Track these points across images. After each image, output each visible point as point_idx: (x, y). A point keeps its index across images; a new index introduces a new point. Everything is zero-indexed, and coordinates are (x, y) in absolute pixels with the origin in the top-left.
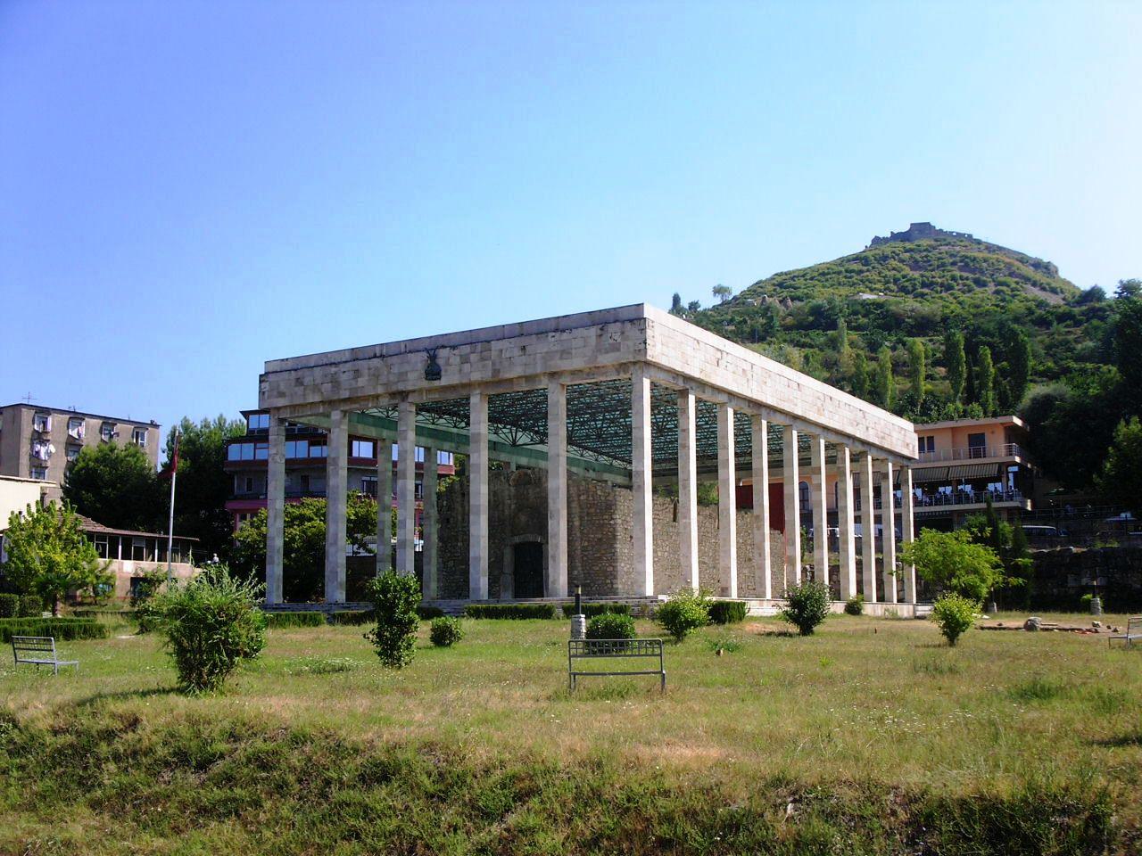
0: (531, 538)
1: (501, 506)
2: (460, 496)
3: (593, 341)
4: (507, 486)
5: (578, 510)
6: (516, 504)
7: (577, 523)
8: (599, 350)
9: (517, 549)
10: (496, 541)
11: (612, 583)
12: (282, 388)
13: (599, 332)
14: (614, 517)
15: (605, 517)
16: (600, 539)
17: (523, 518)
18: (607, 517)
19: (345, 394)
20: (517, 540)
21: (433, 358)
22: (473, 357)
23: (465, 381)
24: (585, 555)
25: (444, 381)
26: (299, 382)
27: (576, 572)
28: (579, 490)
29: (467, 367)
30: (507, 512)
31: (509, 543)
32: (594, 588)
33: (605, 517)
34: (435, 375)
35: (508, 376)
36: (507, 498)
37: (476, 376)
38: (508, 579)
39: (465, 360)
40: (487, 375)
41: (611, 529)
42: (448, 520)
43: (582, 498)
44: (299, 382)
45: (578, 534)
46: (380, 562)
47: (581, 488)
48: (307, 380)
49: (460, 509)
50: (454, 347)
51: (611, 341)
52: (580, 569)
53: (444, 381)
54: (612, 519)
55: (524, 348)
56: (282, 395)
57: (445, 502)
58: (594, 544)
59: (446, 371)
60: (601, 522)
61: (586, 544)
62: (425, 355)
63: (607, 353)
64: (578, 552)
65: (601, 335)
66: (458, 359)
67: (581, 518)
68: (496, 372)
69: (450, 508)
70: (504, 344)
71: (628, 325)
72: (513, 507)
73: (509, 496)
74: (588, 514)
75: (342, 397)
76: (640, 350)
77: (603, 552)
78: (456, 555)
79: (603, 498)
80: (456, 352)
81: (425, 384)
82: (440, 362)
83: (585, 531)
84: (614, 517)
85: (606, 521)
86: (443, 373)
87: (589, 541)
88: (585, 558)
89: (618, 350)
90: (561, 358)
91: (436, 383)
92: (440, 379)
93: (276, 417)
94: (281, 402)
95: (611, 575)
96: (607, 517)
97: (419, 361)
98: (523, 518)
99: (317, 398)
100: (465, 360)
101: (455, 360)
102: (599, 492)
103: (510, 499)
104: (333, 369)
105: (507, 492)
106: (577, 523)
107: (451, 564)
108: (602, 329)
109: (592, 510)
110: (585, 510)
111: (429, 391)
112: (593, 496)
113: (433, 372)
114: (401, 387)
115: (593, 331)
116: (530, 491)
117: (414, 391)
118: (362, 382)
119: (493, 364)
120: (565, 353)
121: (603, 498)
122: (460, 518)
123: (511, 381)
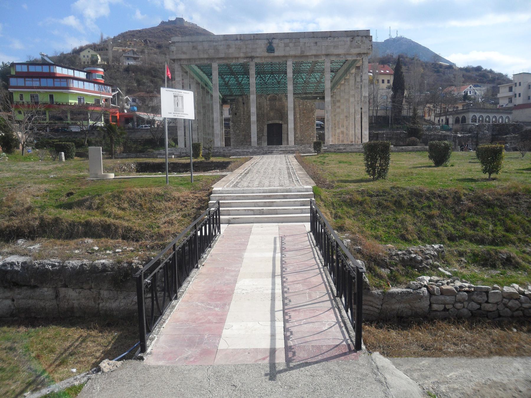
0: (277, 122)
1: (262, 109)
3: (349, 43)
4: (265, 100)
5: (299, 111)
7: (298, 116)
8: (351, 47)
9: (269, 126)
12: (184, 49)
13: (352, 40)
14: (315, 114)
16: (308, 123)
19: (222, 55)
20: (270, 122)
21: (270, 43)
22: (291, 45)
23: (287, 54)
25: (276, 54)
26: (194, 48)
27: (297, 135)
28: (299, 103)
29: (288, 49)
30: (265, 111)
34: (272, 50)
35: (308, 54)
37: (292, 53)
38: (265, 138)
39: (286, 45)
40: (298, 53)
42: (236, 114)
43: (301, 106)
44: (194, 48)
45: (299, 121)
48: (200, 47)
50: (281, 39)
51: (357, 44)
53: (276, 54)
55: (316, 43)
56: (184, 53)
57: (234, 107)
59: (277, 49)
61: (302, 124)
62: (266, 42)
63: (355, 48)
64: (299, 127)
65: (352, 41)
66: (283, 45)
67: (300, 115)
68: (302, 52)
70: (306, 40)
71: (364, 38)
72: (268, 109)
73: (267, 105)
74: (303, 113)
75: (220, 56)
76: (369, 49)
80: (281, 41)
81: (266, 54)
82: (274, 45)
83: (302, 119)
86: (275, 50)
87: (303, 123)
89: (360, 48)
90: (334, 49)
91: (272, 54)
92: (274, 52)
93: (179, 63)
94: (183, 56)
97: (262, 44)
98: (272, 114)
99: (206, 56)
100: (286, 45)
101: (282, 45)
102: (308, 104)
104: (215, 44)
105: (265, 103)
106: (298, 116)
107: (238, 131)
108: (353, 38)
109: (305, 111)
110: (302, 111)
111: (265, 57)
112: (305, 106)
113: (270, 49)
114: (253, 54)
115: (349, 39)
116: (277, 103)
117: (257, 57)
118: (231, 51)
119: (301, 48)
120: (336, 47)
122: (242, 113)
123: (307, 56)
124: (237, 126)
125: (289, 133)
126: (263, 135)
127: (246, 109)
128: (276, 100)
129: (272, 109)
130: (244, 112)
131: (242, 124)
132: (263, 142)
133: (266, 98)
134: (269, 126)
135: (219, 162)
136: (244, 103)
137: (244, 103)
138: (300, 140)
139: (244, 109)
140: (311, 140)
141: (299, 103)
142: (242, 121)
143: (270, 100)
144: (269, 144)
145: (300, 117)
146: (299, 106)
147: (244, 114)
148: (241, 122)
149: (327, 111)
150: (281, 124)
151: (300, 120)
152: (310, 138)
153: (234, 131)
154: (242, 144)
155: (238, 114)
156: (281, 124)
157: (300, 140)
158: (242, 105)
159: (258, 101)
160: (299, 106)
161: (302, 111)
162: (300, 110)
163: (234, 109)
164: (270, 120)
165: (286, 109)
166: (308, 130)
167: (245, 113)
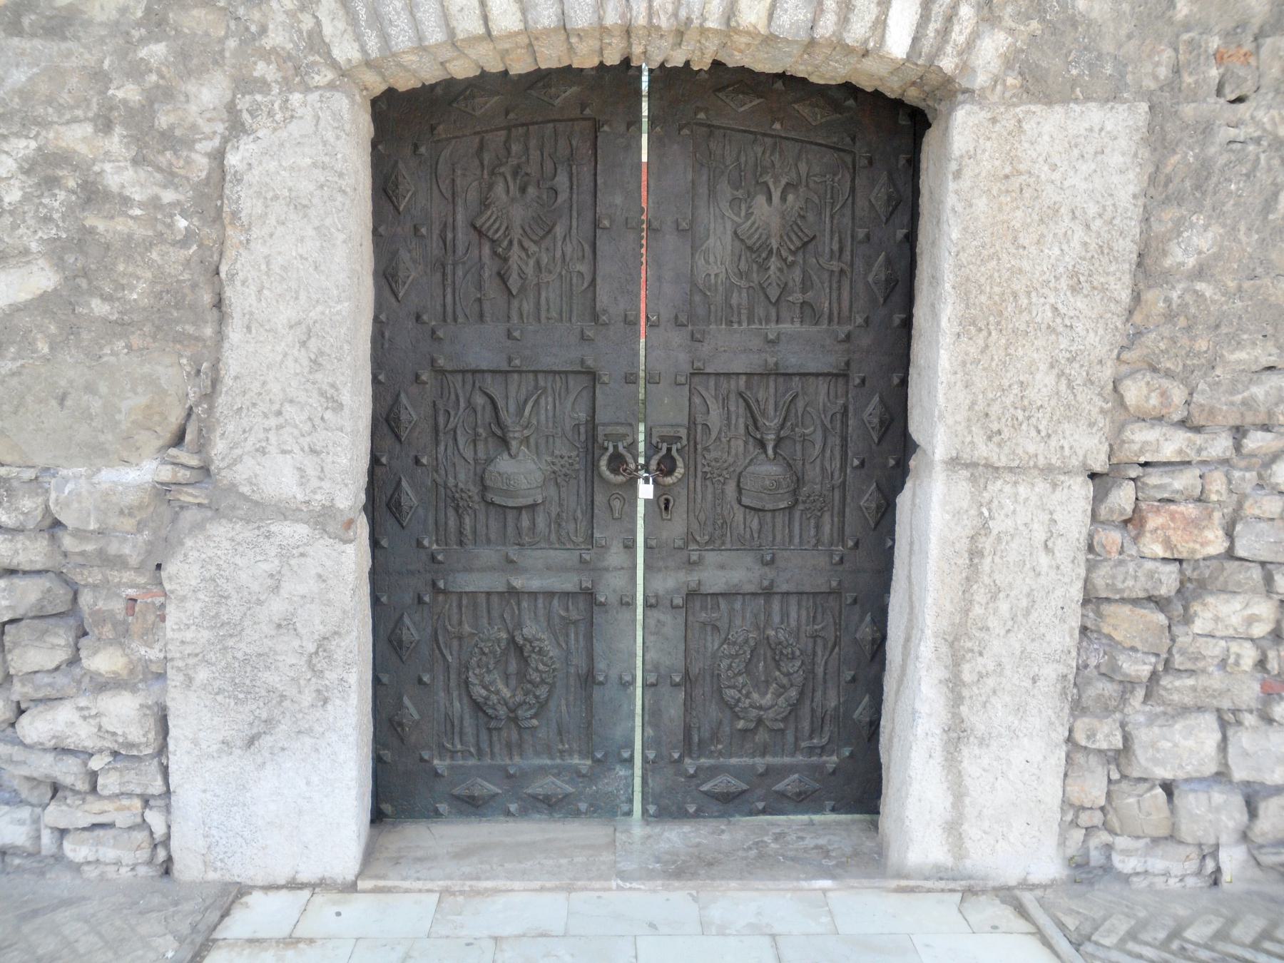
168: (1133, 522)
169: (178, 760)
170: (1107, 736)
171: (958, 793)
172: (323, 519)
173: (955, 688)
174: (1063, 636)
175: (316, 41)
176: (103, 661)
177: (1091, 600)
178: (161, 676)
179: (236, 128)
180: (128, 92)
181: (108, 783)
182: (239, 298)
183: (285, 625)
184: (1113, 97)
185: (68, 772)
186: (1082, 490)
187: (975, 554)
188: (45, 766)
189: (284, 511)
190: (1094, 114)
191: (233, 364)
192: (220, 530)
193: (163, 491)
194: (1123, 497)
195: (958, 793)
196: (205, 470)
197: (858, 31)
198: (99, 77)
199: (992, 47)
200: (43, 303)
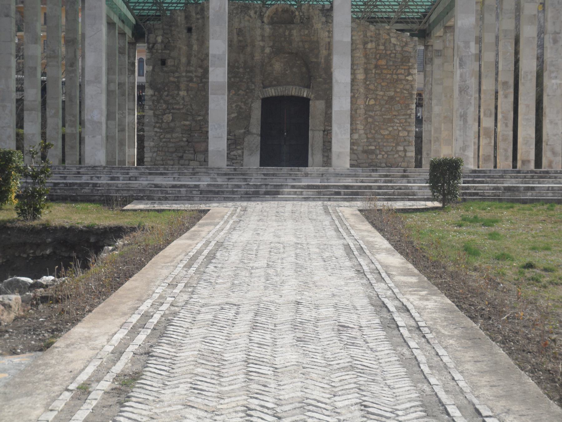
0: (293, 91)
1: (249, 49)
2: (185, 31)
4: (259, 23)
6: (272, 47)
10: (241, 92)
11: (405, 151)
15: (399, 71)
16: (392, 98)
17: (278, 66)
18: (403, 71)
20: (272, 92)
24: (371, 117)
28: (365, 36)
30: (257, 57)
31: (261, 97)
32: (380, 156)
33: (399, 71)
36: (259, 38)
38: (254, 140)
41: (408, 87)
42: (163, 63)
43: (369, 46)
45: (362, 90)
46: (28, 110)
47: (369, 34)
49: (184, 48)
52: (362, 132)
54: (409, 74)
57: (159, 39)
58: (383, 102)
60: (395, 77)
61: (372, 102)
67: (366, 71)
69: (167, 46)
72: (267, 50)
73: (263, 36)
74: (376, 67)
77: (394, 113)
78: (177, 107)
79: (398, 49)
83: (372, 87)
84: (412, 71)
85: (401, 77)
87: (375, 99)
88: (370, 120)
95: (405, 140)
96: (403, 71)
98: (278, 66)
102: (393, 40)
103: (263, 40)
105: (258, 32)
107: (168, 117)
109: (383, 62)
110: (374, 62)
112: (384, 44)
116: (294, 32)
121: (398, 49)
122: (184, 60)
124: (166, 102)
125: (335, 128)
126: (248, 132)
127: (195, 47)
128: (292, 22)
129: (277, 51)
130: (189, 56)
131: (182, 93)
132: (246, 153)
133: (261, 17)
134: (267, 103)
135: (71, 230)
136: (189, 30)
137: (189, 30)
138: (365, 152)
139: (190, 46)
140: (397, 152)
141: (365, 36)
142: (183, 86)
143: (272, 22)
144: (264, 162)
145: (366, 79)
146: (365, 43)
147: (189, 63)
148: (179, 89)
149: (461, 60)
150: (306, 102)
151: (367, 89)
152: (398, 144)
153: (155, 115)
154: (181, 157)
155: (169, 62)
156: (306, 102)
157: (365, 152)
158: (184, 34)
159: (236, 25)
160: (365, 43)
161: (374, 62)
162: (366, 56)
163: (159, 46)
164: (271, 86)
165: (324, 52)
166: (390, 120)
167: (194, 61)
168: (327, 135)
169: (244, 156)
170: (326, 154)
171: (313, 160)
172: (258, 135)
173: (312, 150)
174: (321, 145)
175: (259, 96)
176: (238, 147)
177: (324, 142)
178: (243, 149)
179: (252, 103)
180: (244, 100)
181: (238, 158)
182: (252, 116)
183: (254, 144)
184: (323, 100)
185: (235, 157)
186: (322, 132)
187: (313, 138)
188: (233, 157)
189: (254, 134)
190: (321, 101)
191: (251, 121)
192: (249, 136)
193: (245, 132)
194: (326, 133)
195: (313, 160)
196: (248, 131)
197: (302, 95)
198: (242, 99)
199: (313, 96)
200: (235, 117)
